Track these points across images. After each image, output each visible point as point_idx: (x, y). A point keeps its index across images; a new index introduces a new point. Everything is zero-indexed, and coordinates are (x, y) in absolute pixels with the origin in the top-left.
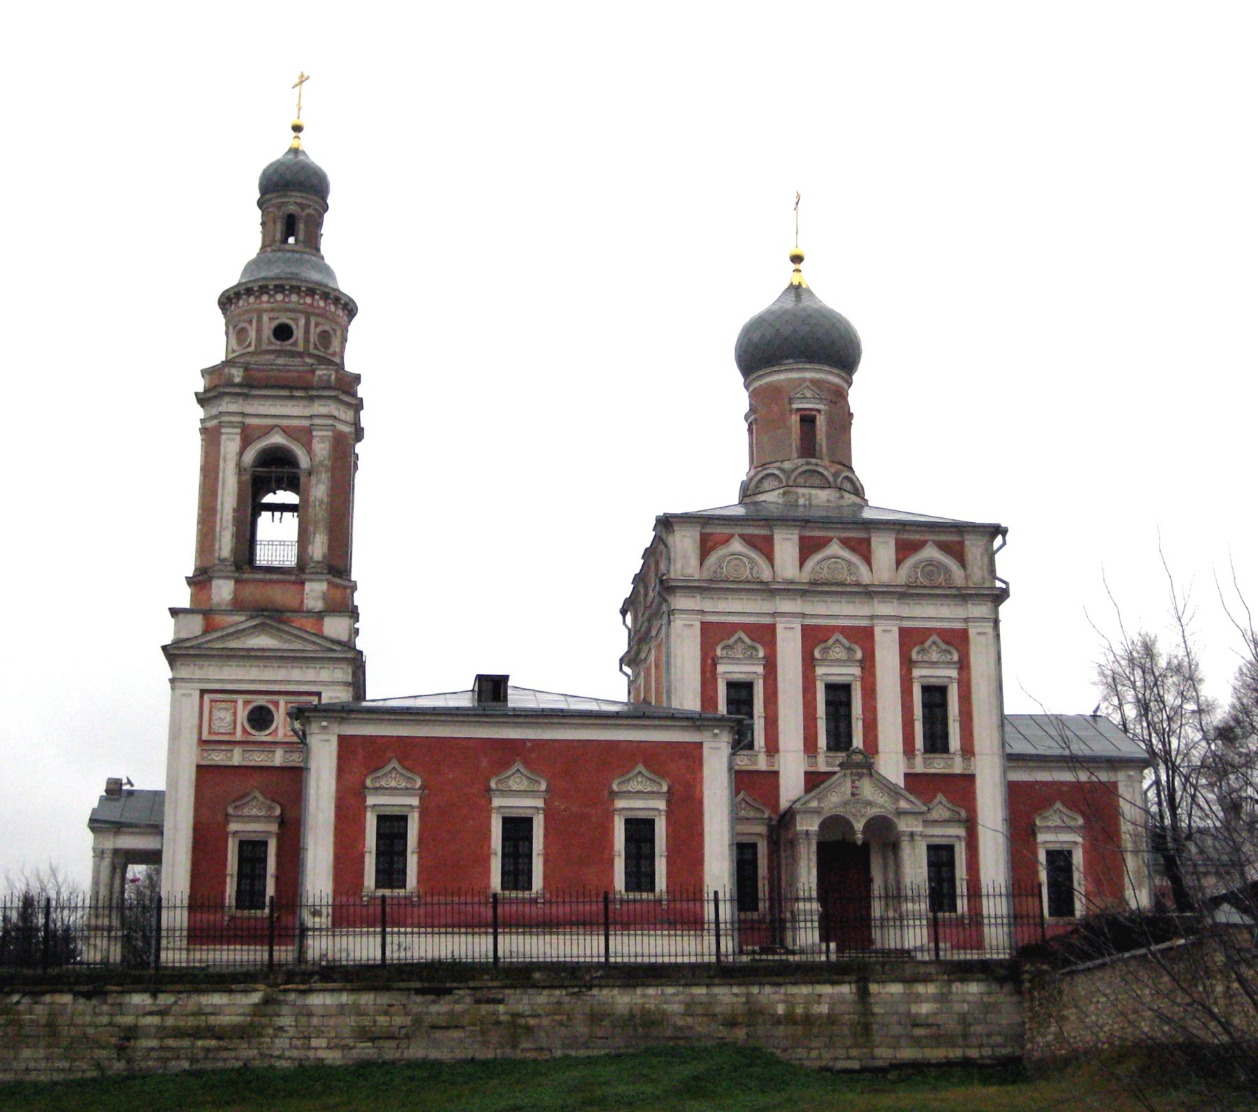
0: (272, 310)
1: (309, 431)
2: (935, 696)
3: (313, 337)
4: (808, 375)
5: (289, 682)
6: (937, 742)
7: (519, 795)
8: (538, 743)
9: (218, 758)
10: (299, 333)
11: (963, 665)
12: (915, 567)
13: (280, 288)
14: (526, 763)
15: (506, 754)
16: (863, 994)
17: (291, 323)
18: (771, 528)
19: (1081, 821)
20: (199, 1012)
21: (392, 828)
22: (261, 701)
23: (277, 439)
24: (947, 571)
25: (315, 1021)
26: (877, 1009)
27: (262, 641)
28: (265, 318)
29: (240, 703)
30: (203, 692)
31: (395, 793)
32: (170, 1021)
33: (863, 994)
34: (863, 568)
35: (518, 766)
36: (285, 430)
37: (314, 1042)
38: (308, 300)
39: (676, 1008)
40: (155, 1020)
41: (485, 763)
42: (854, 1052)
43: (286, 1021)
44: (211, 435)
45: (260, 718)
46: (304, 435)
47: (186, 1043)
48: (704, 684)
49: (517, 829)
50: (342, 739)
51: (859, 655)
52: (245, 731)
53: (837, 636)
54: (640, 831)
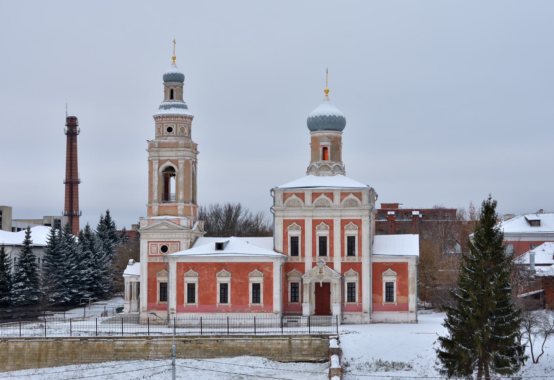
1: (177, 161)
2: (351, 240)
3: (179, 130)
4: (325, 134)
6: (351, 252)
7: (224, 278)
9: (153, 260)
10: (174, 129)
11: (360, 229)
12: (347, 201)
14: (226, 269)
15: (221, 266)
16: (290, 342)
17: (172, 127)
19: (396, 274)
20: (132, 346)
21: (191, 287)
22: (164, 244)
23: (169, 164)
24: (356, 201)
25: (159, 348)
26: (293, 347)
28: (164, 125)
29: (159, 245)
30: (148, 242)
31: (191, 278)
32: (125, 348)
33: (290, 342)
34: (331, 202)
35: (223, 270)
36: (171, 161)
37: (159, 353)
38: (177, 119)
39: (244, 346)
40: (122, 348)
41: (215, 269)
42: (287, 357)
43: (152, 348)
44: (151, 162)
46: (176, 162)
47: (129, 353)
48: (284, 238)
49: (224, 287)
50: (177, 263)
51: (329, 228)
52: (160, 252)
53: (322, 223)
54: (256, 287)
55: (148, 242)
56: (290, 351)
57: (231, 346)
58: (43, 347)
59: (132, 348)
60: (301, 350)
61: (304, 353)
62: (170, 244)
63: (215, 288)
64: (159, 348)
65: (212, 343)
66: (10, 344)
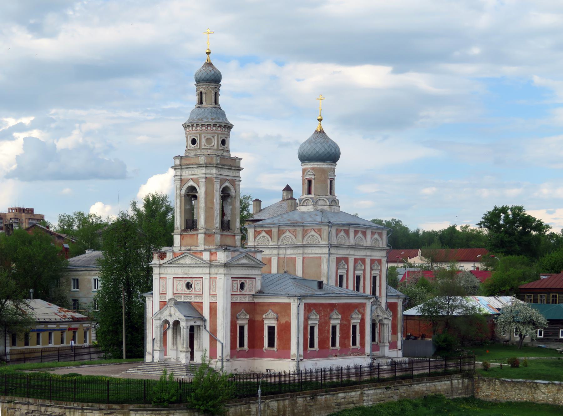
0: (221, 134)
5: (252, 275)
8: (339, 304)
13: (220, 126)
16: (452, 383)
18: (349, 227)
22: (243, 280)
27: (244, 261)
33: (452, 383)
39: (425, 389)
41: (329, 310)
45: (242, 286)
55: (232, 278)
56: (452, 391)
57: (416, 390)
59: (351, 400)
60: (458, 389)
61: (459, 392)
62: (247, 280)
63: (328, 331)
64: (370, 398)
65: (405, 388)
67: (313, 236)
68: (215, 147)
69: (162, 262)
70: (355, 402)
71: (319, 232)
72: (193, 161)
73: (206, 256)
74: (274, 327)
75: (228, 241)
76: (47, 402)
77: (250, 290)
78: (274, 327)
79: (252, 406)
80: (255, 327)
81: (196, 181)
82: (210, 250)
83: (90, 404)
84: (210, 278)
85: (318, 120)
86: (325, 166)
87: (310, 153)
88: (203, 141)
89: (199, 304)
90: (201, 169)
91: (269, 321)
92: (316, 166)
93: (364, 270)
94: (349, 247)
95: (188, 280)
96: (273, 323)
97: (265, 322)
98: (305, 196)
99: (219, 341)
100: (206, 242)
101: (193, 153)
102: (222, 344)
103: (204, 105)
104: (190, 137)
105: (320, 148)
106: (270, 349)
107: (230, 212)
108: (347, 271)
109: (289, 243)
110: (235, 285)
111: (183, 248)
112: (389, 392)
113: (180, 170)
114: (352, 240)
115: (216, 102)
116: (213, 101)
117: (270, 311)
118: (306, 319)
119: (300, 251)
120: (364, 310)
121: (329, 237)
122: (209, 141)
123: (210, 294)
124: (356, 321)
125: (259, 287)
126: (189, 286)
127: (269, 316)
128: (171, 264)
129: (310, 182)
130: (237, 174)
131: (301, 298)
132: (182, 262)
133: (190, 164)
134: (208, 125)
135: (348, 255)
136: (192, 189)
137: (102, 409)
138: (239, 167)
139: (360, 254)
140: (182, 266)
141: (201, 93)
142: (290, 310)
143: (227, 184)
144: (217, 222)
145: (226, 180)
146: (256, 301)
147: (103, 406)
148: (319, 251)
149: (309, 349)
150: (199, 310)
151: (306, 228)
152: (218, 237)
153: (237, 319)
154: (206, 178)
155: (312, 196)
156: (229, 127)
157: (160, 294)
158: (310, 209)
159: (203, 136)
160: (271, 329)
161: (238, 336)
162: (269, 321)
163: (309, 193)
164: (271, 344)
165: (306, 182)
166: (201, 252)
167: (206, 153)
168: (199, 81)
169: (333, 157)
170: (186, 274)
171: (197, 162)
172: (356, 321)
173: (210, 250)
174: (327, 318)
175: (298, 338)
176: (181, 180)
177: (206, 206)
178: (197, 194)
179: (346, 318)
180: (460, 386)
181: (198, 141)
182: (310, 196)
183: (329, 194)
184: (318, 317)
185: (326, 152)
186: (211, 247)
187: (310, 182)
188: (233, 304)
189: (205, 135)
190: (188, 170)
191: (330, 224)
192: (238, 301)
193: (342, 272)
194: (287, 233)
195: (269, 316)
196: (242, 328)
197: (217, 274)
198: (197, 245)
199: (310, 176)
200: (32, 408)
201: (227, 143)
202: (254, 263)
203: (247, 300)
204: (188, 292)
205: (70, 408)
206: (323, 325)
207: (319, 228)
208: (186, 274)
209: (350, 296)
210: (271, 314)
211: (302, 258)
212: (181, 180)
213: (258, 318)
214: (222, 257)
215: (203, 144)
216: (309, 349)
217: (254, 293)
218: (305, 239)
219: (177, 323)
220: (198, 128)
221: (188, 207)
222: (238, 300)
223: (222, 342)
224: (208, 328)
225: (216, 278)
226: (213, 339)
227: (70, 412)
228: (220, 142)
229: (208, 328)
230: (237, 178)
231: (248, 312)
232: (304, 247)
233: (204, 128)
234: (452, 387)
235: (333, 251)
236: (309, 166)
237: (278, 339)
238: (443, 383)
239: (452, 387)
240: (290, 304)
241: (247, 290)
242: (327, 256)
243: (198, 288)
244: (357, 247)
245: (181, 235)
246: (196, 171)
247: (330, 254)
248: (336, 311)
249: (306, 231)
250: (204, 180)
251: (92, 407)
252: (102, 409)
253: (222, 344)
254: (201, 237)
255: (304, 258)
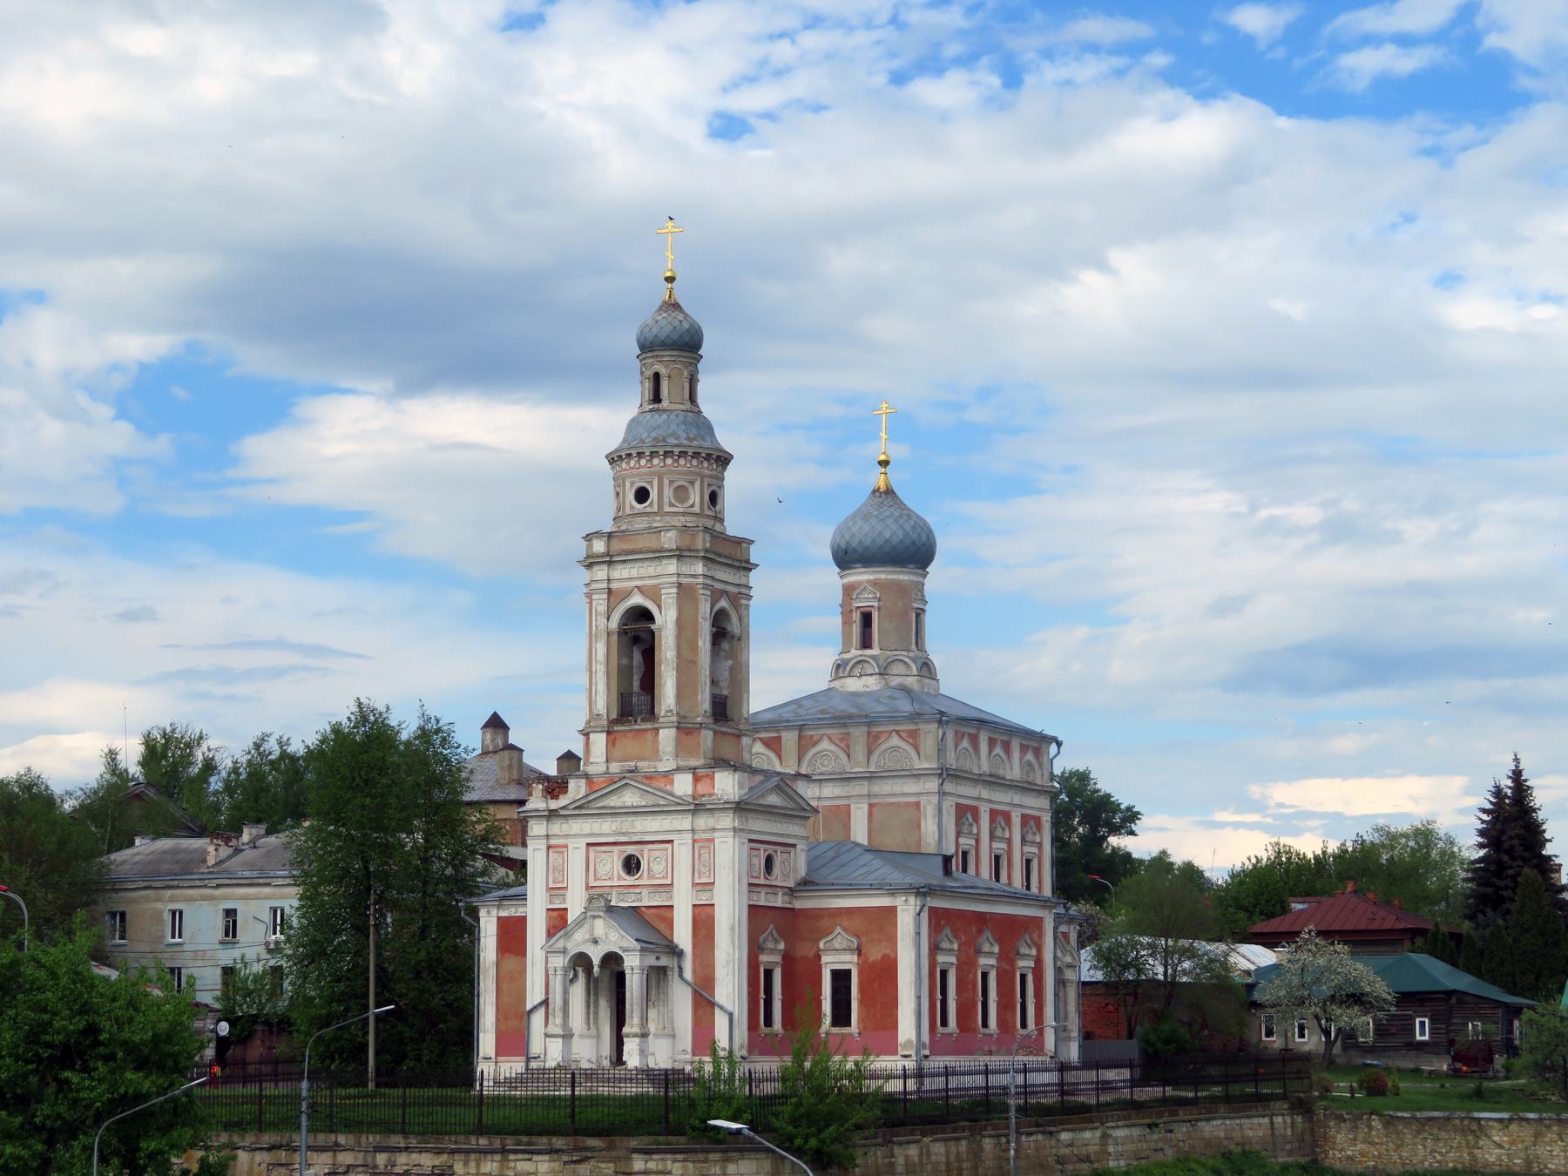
5: (789, 836)
16: (1272, 1123)
18: (979, 730)
27: (774, 799)
33: (1272, 1123)
39: (1222, 1135)
40: (1067, 1151)
57: (1207, 1135)
58: (952, 1157)
61: (1288, 1147)
62: (779, 849)
66: (897, 1150)
67: (895, 748)
68: (697, 509)
69: (554, 805)
70: (1093, 1157)
71: (913, 738)
72: (641, 543)
73: (683, 785)
74: (848, 972)
75: (727, 751)
76: (397, 1140)
77: (786, 876)
78: (848, 972)
79: (897, 1150)
80: (800, 974)
81: (654, 593)
82: (693, 770)
83: (525, 1139)
84: (694, 841)
85: (880, 463)
86: (904, 576)
87: (867, 543)
88: (668, 493)
89: (662, 912)
90: (665, 562)
91: (836, 956)
92: (883, 576)
93: (1009, 842)
94: (979, 780)
95: (631, 850)
96: (848, 961)
97: (825, 959)
98: (854, 652)
99: (721, 1008)
100: (680, 749)
101: (640, 524)
102: (731, 1015)
103: (665, 404)
104: (632, 484)
105: (889, 531)
106: (835, 1030)
107: (727, 674)
108: (977, 841)
109: (829, 769)
110: (755, 861)
111: (615, 768)
112: (1155, 1137)
113: (605, 567)
114: (983, 764)
115: (692, 398)
116: (687, 396)
117: (838, 930)
118: (935, 949)
119: (861, 788)
120: (1041, 936)
121: (941, 751)
122: (681, 493)
123: (694, 885)
124: (1025, 964)
125: (802, 871)
126: (632, 865)
127: (836, 944)
128: (581, 809)
129: (867, 619)
130: (743, 581)
131: (922, 892)
132: (613, 801)
133: (633, 552)
134: (683, 454)
135: (978, 799)
136: (643, 615)
137: (557, 1151)
138: (748, 561)
139: (1003, 798)
140: (614, 813)
141: (657, 376)
142: (895, 924)
143: (723, 603)
144: (704, 703)
145: (725, 593)
146: (798, 904)
147: (559, 1142)
148: (911, 787)
149: (940, 1029)
150: (662, 927)
151: (875, 729)
152: (707, 736)
153: (761, 949)
154: (680, 585)
155: (875, 651)
156: (723, 459)
157: (549, 889)
158: (872, 683)
159: (666, 482)
160: (841, 978)
161: (762, 995)
162: (836, 956)
163: (866, 643)
164: (841, 1016)
165: (857, 617)
166: (668, 775)
167: (679, 521)
168: (648, 347)
169: (916, 553)
170: (624, 834)
171: (654, 545)
172: (1025, 964)
173: (693, 770)
174: (971, 951)
175: (919, 998)
176: (610, 591)
177: (679, 656)
178: (653, 627)
179: (1008, 957)
180: (1289, 1132)
181: (654, 495)
182: (868, 652)
183: (913, 647)
184: (956, 946)
185: (908, 542)
186: (693, 763)
187: (867, 619)
188: (753, 909)
189: (672, 477)
190: (629, 565)
191: (942, 718)
192: (762, 903)
193: (967, 842)
194: (825, 745)
195: (836, 944)
196: (769, 974)
197: (714, 829)
198: (655, 755)
199: (865, 601)
200: (346, 1158)
201: (719, 501)
202: (791, 805)
203: (779, 901)
204: (630, 880)
205: (468, 1152)
206: (966, 965)
207: (912, 727)
208: (624, 834)
209: (1014, 898)
210: (840, 938)
211: (865, 807)
212: (610, 591)
213: (804, 950)
214: (726, 785)
215: (666, 500)
216: (940, 1029)
217: (791, 884)
218: (874, 758)
219: (612, 960)
220: (656, 461)
221: (625, 661)
222: (762, 900)
223: (730, 1008)
224: (688, 974)
225: (712, 840)
226: (704, 1003)
227: (466, 1163)
228: (707, 498)
229: (688, 974)
230: (743, 590)
231: (783, 934)
232: (871, 777)
233: (669, 461)
234: (1273, 1135)
235: (948, 787)
236: (861, 576)
237: (861, 1002)
238: (1255, 1121)
239: (1273, 1135)
240: (892, 910)
241: (777, 878)
242: (935, 799)
243: (658, 868)
244: (994, 781)
245: (609, 733)
246: (650, 569)
247: (942, 794)
248: (988, 934)
249: (877, 737)
250: (675, 590)
251: (529, 1144)
252: (557, 1151)
253: (731, 1015)
254: (667, 736)
255: (871, 806)
